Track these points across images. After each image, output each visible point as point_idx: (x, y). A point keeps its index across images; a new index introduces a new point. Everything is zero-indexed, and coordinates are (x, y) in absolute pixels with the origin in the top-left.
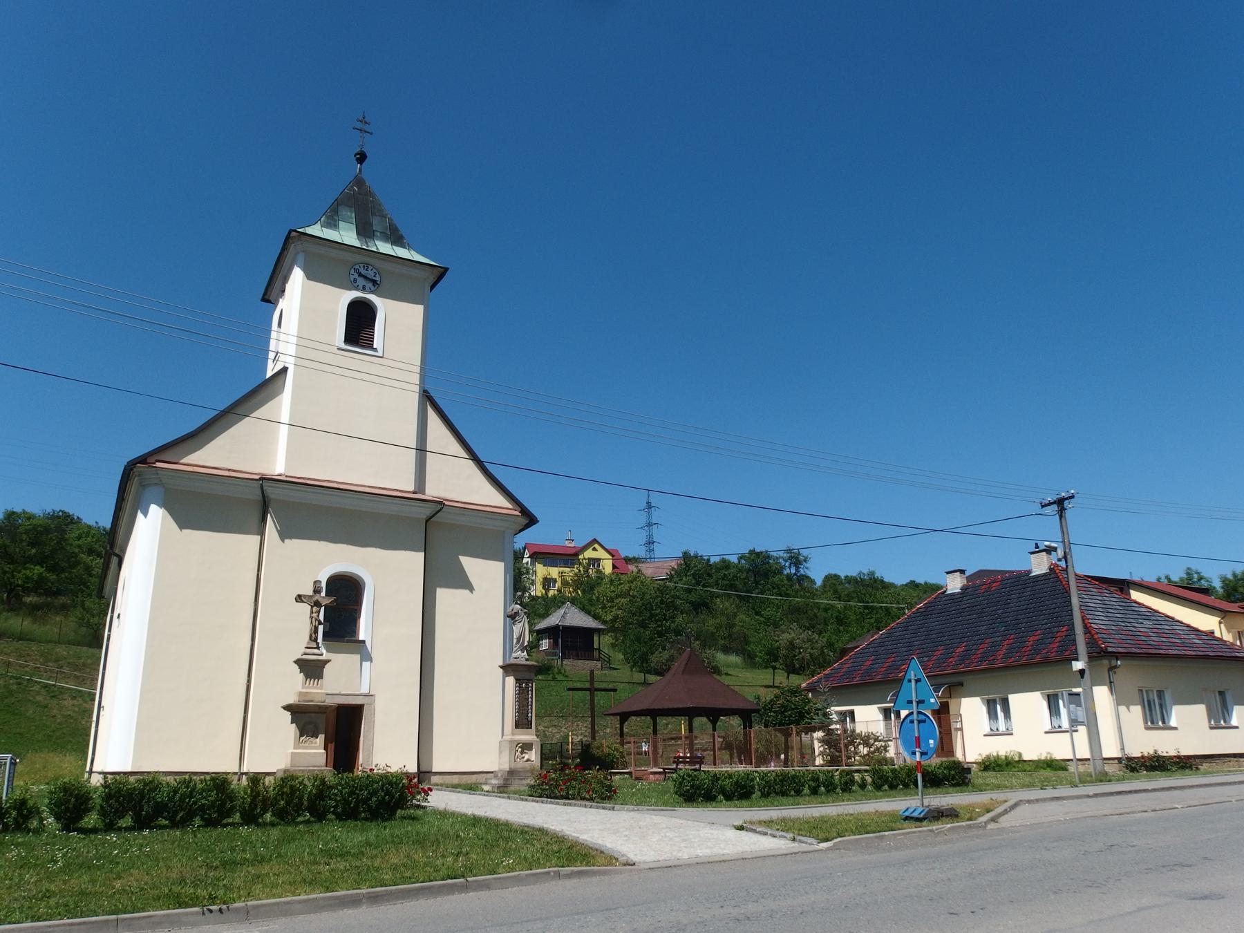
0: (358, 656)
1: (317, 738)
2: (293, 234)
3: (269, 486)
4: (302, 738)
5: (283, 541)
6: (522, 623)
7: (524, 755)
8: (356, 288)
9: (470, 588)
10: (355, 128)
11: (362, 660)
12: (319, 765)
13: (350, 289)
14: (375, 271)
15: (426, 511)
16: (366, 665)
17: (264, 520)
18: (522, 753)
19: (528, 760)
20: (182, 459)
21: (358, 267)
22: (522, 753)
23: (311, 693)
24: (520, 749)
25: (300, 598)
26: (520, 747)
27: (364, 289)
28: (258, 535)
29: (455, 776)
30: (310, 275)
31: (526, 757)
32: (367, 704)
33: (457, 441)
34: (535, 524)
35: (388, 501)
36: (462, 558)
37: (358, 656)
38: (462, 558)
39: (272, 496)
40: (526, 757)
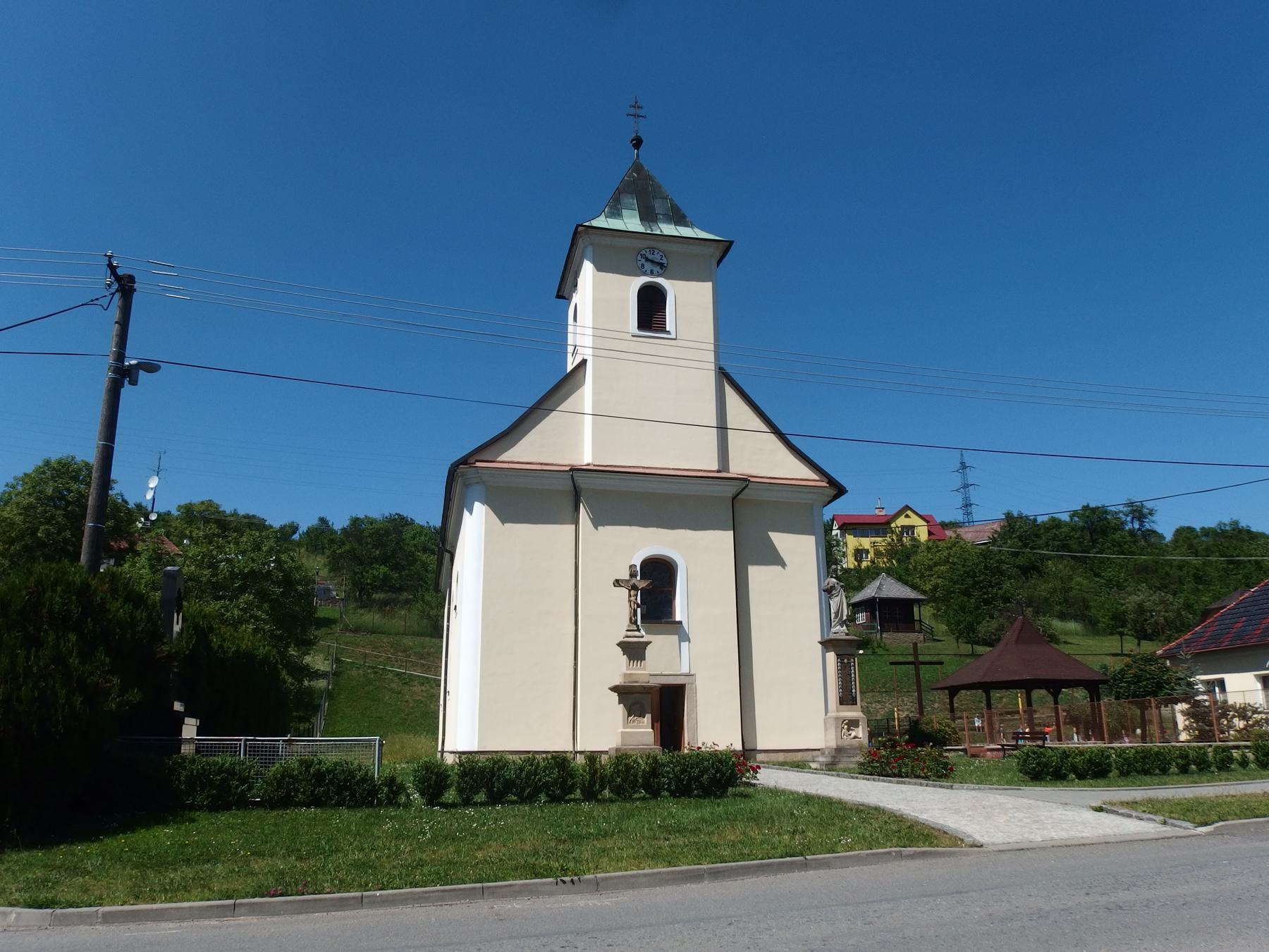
0: (677, 637)
1: (644, 717)
2: (580, 229)
3: (578, 477)
4: (630, 718)
7: (850, 732)
8: (645, 274)
9: (783, 565)
14: (661, 254)
15: (731, 490)
16: (685, 645)
17: (577, 509)
18: (849, 730)
19: (855, 737)
22: (849, 730)
23: (635, 674)
25: (617, 583)
26: (846, 724)
27: (652, 273)
28: (573, 524)
30: (600, 267)
31: (853, 734)
32: (688, 684)
33: (758, 416)
34: (844, 494)
36: (770, 534)
37: (677, 637)
38: (770, 534)
39: (582, 486)
40: (853, 734)
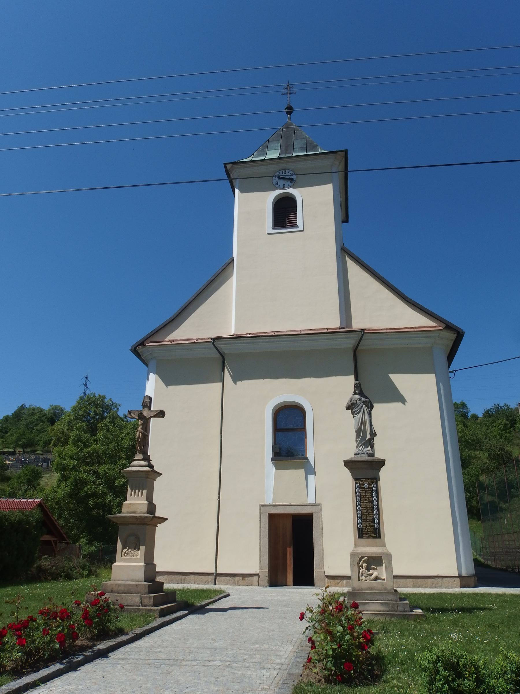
0: (303, 470)
1: (138, 550)
2: (229, 166)
3: (222, 344)
4: (125, 550)
5: (236, 384)
6: (361, 414)
7: (371, 572)
8: (278, 188)
9: (403, 400)
10: (282, 95)
11: (306, 475)
12: (137, 579)
13: (274, 190)
14: (292, 172)
15: (350, 342)
16: (311, 478)
17: (223, 370)
18: (368, 569)
19: (377, 578)
20: (165, 338)
21: (279, 174)
22: (368, 569)
23: (134, 504)
24: (365, 565)
25: (161, 414)
26: (365, 562)
27: (284, 187)
28: (221, 382)
29: (408, 580)
30: (242, 191)
31: (375, 574)
32: (315, 513)
33: (377, 280)
34: (463, 335)
35: (314, 338)
36: (392, 376)
37: (303, 470)
38: (392, 376)
39: (226, 351)
40: (375, 574)
